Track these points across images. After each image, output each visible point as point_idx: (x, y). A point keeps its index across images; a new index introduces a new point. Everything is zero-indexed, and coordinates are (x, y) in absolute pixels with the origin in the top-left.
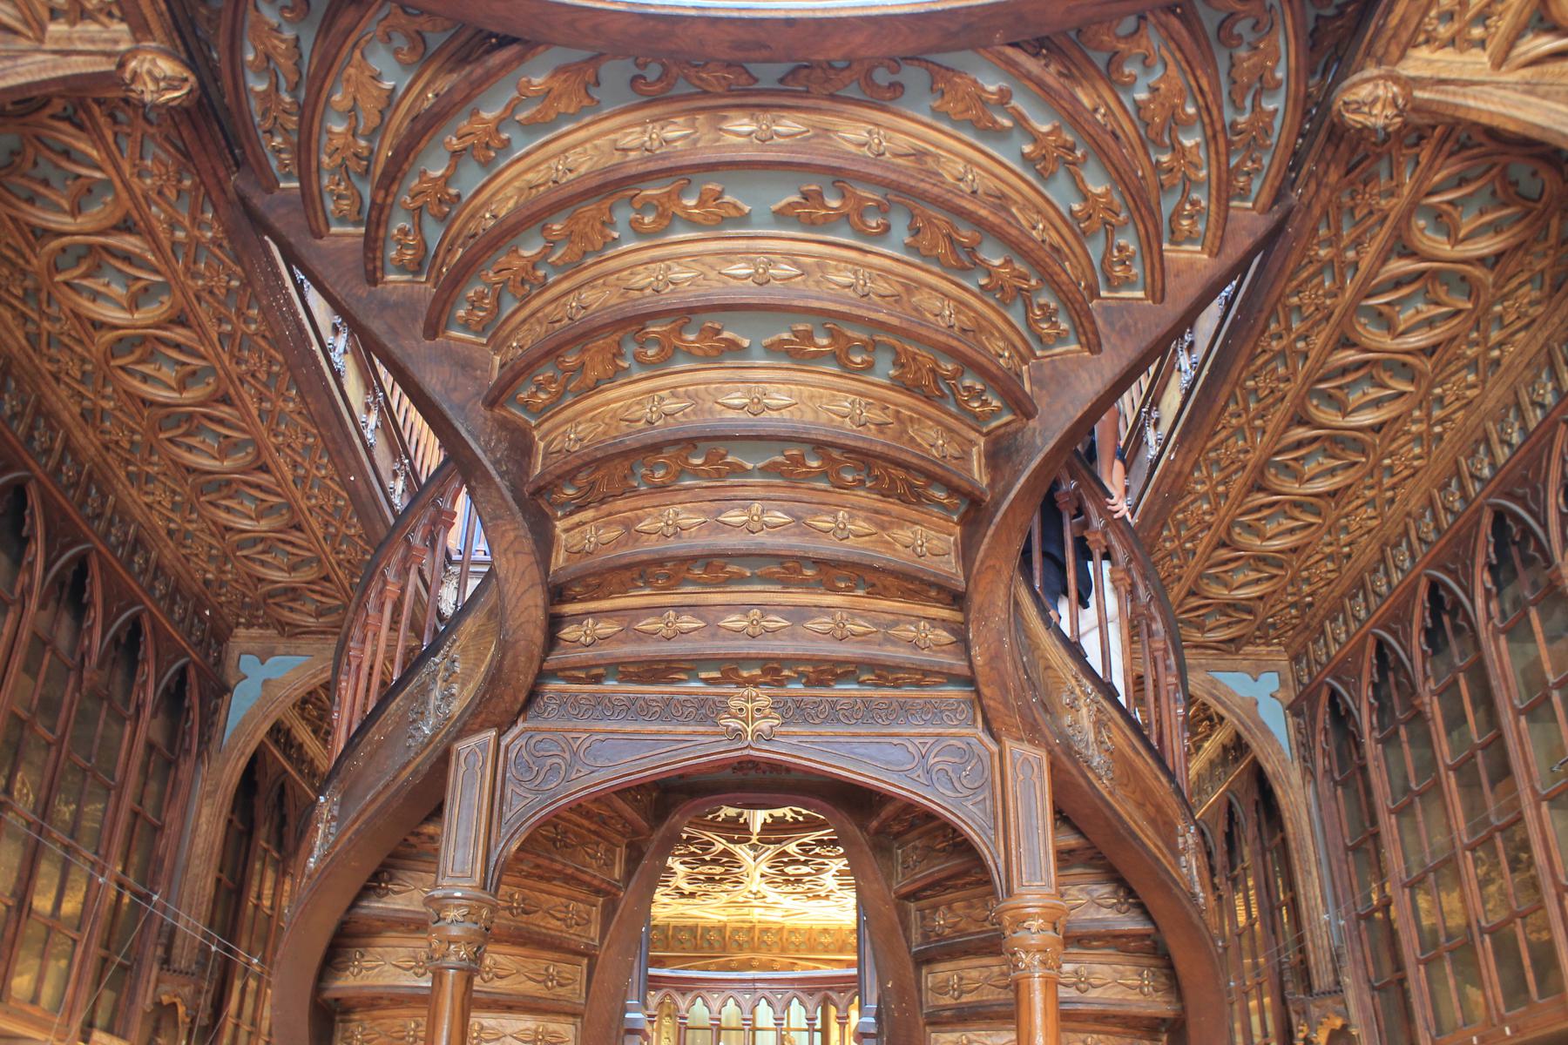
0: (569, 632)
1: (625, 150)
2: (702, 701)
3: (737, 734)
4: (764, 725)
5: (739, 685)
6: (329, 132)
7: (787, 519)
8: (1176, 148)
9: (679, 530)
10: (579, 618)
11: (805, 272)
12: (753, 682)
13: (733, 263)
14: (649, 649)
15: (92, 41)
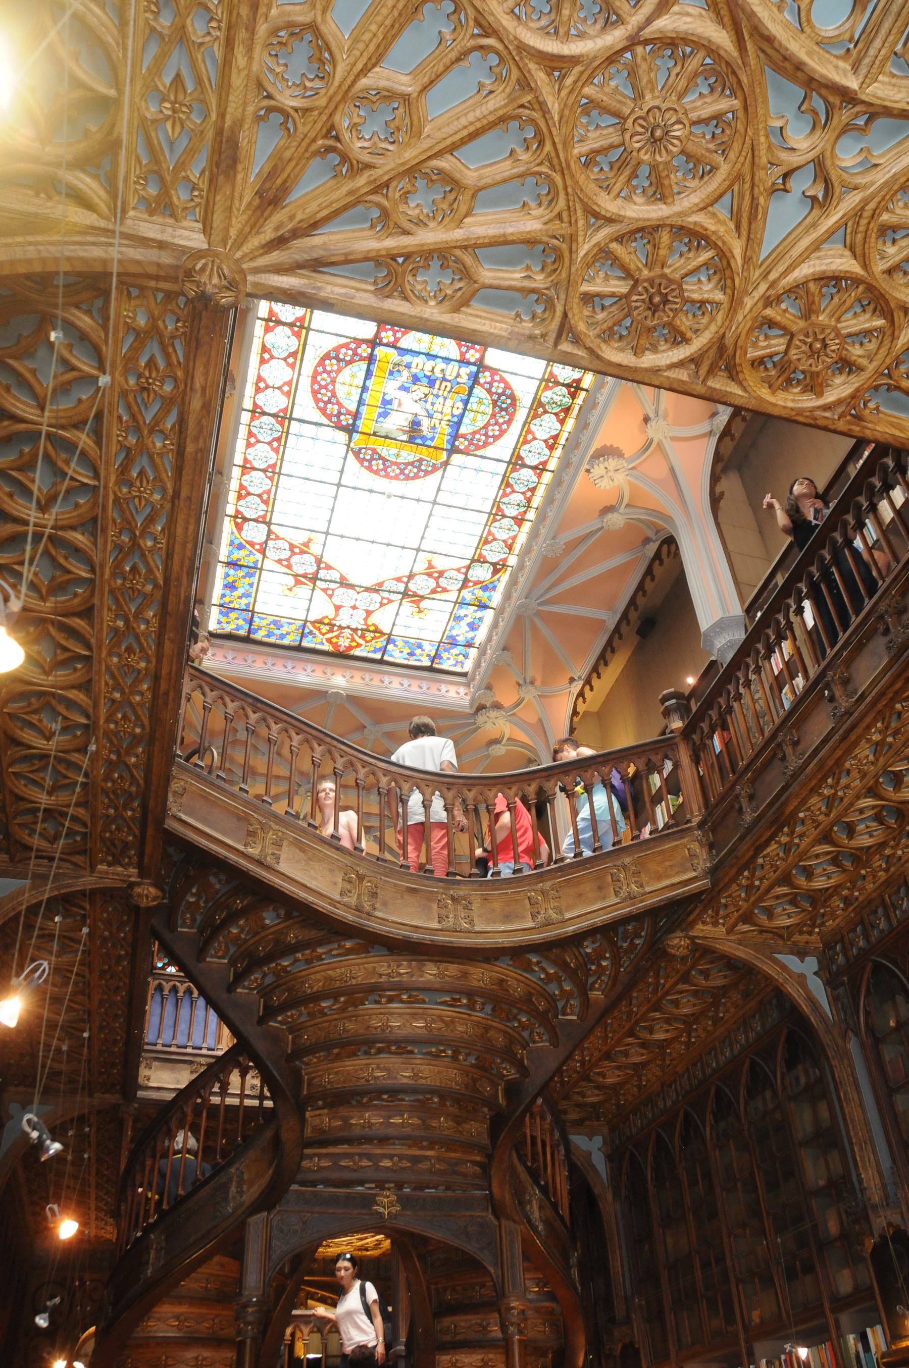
0: (305, 1164)
1: (380, 975)
2: (363, 1196)
3: (381, 1215)
4: (393, 1210)
5: (383, 1189)
6: (230, 932)
7: (419, 1122)
8: (599, 965)
9: (370, 1125)
10: (311, 1157)
11: (447, 1025)
12: (389, 1189)
13: (417, 1020)
14: (347, 1175)
15: (118, 875)
